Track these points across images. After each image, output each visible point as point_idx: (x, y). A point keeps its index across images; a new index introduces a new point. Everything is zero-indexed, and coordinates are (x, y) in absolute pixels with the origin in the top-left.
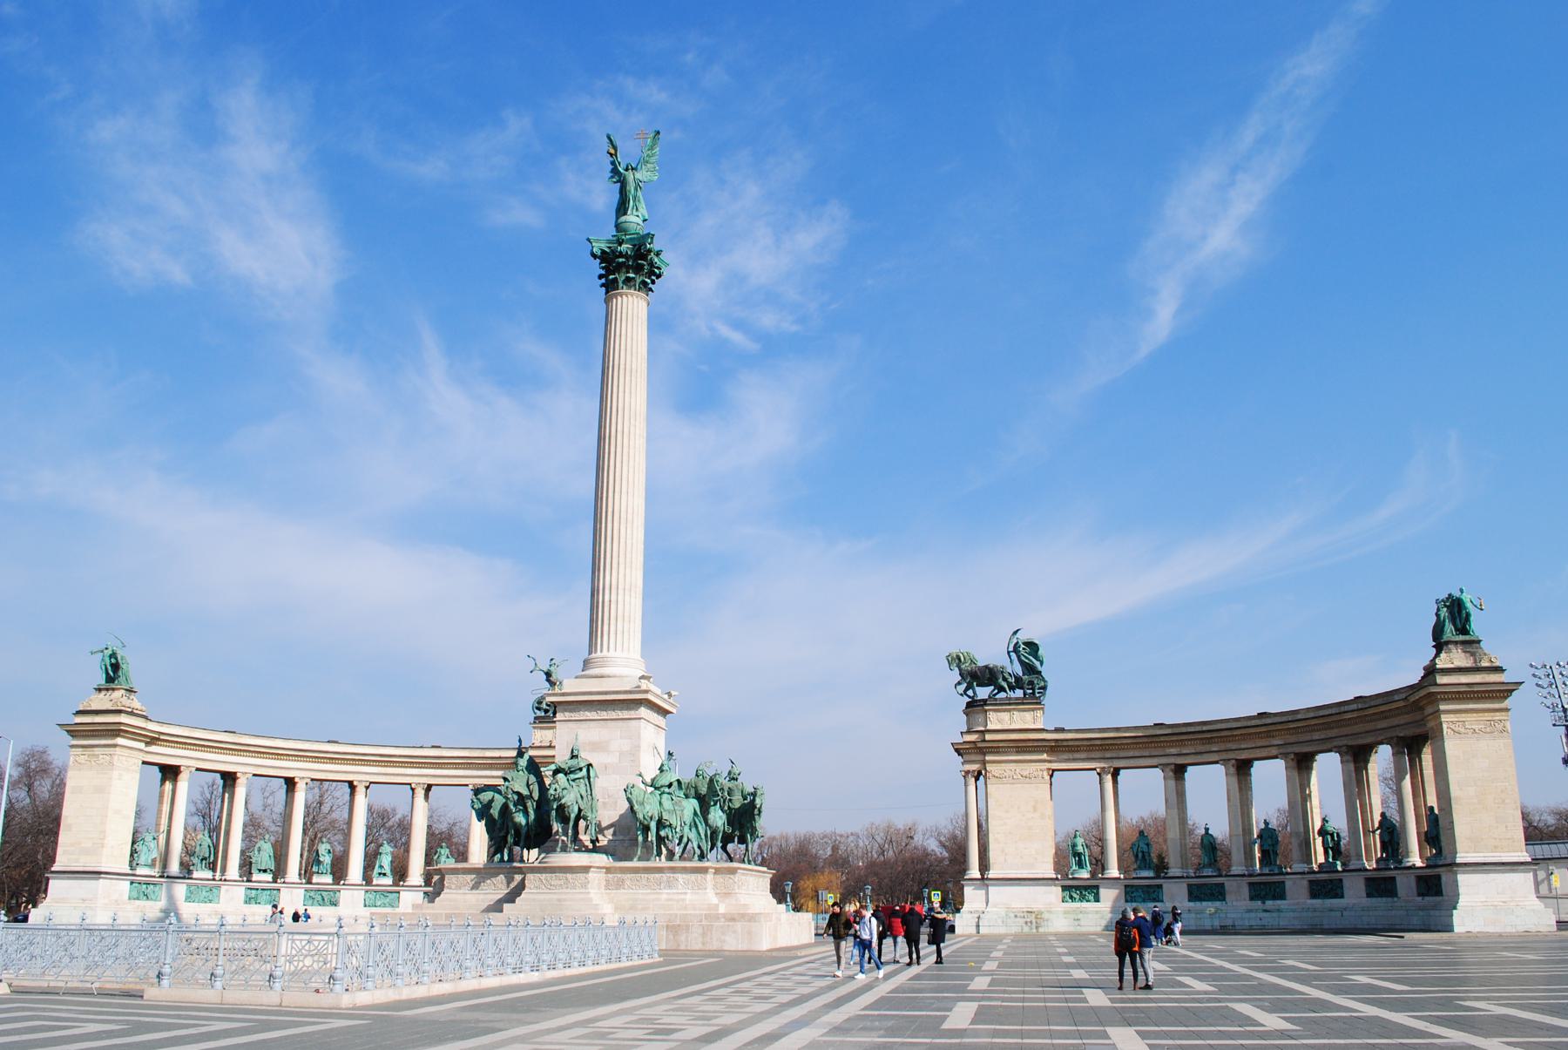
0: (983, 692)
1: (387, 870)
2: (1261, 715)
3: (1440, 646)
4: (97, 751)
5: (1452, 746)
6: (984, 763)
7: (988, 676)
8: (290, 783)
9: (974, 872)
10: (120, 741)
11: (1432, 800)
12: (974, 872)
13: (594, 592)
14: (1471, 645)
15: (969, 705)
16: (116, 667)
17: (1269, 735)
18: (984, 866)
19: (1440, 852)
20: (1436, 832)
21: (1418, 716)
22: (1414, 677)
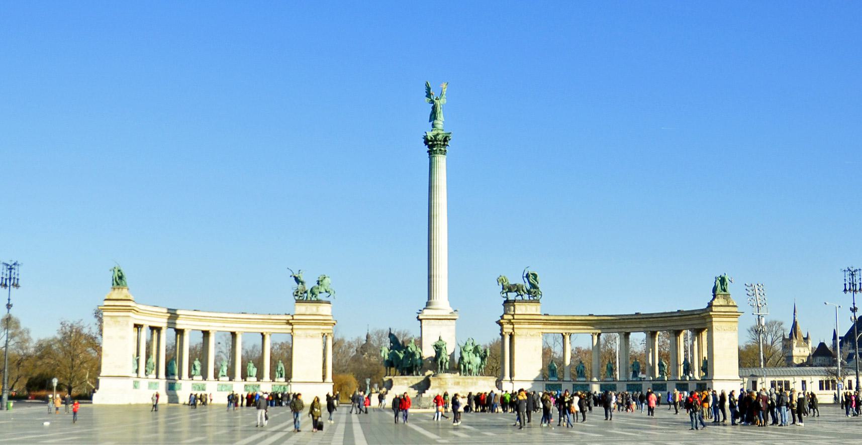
0: (512, 296)
1: (225, 373)
2: (637, 314)
3: (715, 296)
4: (119, 319)
5: (716, 335)
6: (513, 329)
7: (517, 289)
8: (234, 334)
9: (507, 377)
10: (130, 314)
11: (705, 354)
12: (507, 377)
13: (430, 277)
14: (726, 297)
15: (505, 302)
16: (121, 278)
17: (640, 323)
18: (512, 374)
19: (707, 374)
20: (707, 367)
21: (703, 321)
22: (705, 306)
